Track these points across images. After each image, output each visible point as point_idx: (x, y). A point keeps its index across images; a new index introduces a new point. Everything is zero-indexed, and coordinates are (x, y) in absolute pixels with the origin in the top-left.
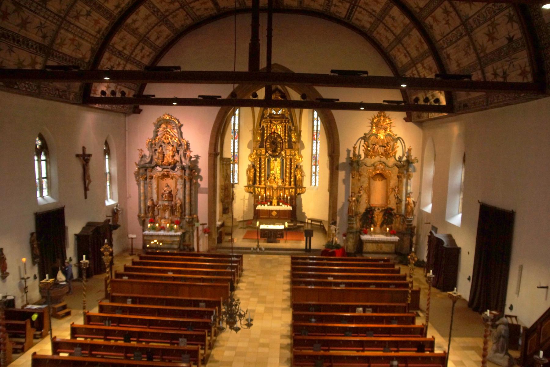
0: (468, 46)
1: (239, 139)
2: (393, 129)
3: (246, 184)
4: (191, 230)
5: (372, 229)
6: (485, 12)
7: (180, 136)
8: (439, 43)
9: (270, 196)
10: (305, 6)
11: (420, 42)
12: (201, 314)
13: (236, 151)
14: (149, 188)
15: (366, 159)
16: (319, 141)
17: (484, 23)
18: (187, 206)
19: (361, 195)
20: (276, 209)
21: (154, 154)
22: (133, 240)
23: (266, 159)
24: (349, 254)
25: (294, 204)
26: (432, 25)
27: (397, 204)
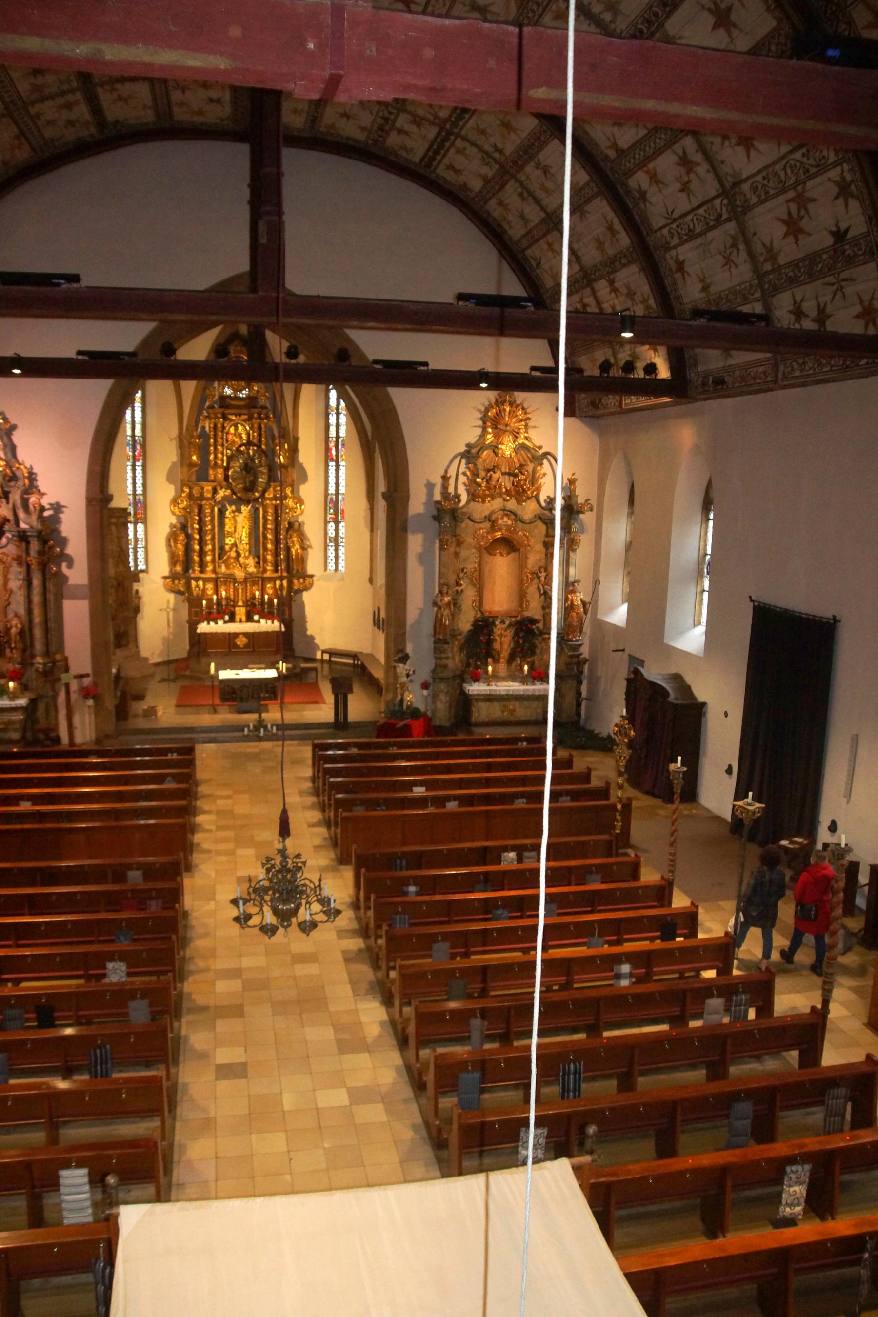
0: (734, 245)
1: (145, 460)
2: (532, 434)
3: (166, 573)
4: (50, 693)
5: (490, 668)
6: (785, 168)
7: (10, 455)
8: (659, 234)
9: (228, 598)
10: (323, 129)
11: (611, 228)
12: (140, 899)
13: (139, 491)
16: (342, 463)
17: (777, 195)
18: (38, 633)
19: (462, 591)
20: (244, 630)
23: (216, 509)
24: (440, 730)
25: (287, 616)
26: (645, 192)
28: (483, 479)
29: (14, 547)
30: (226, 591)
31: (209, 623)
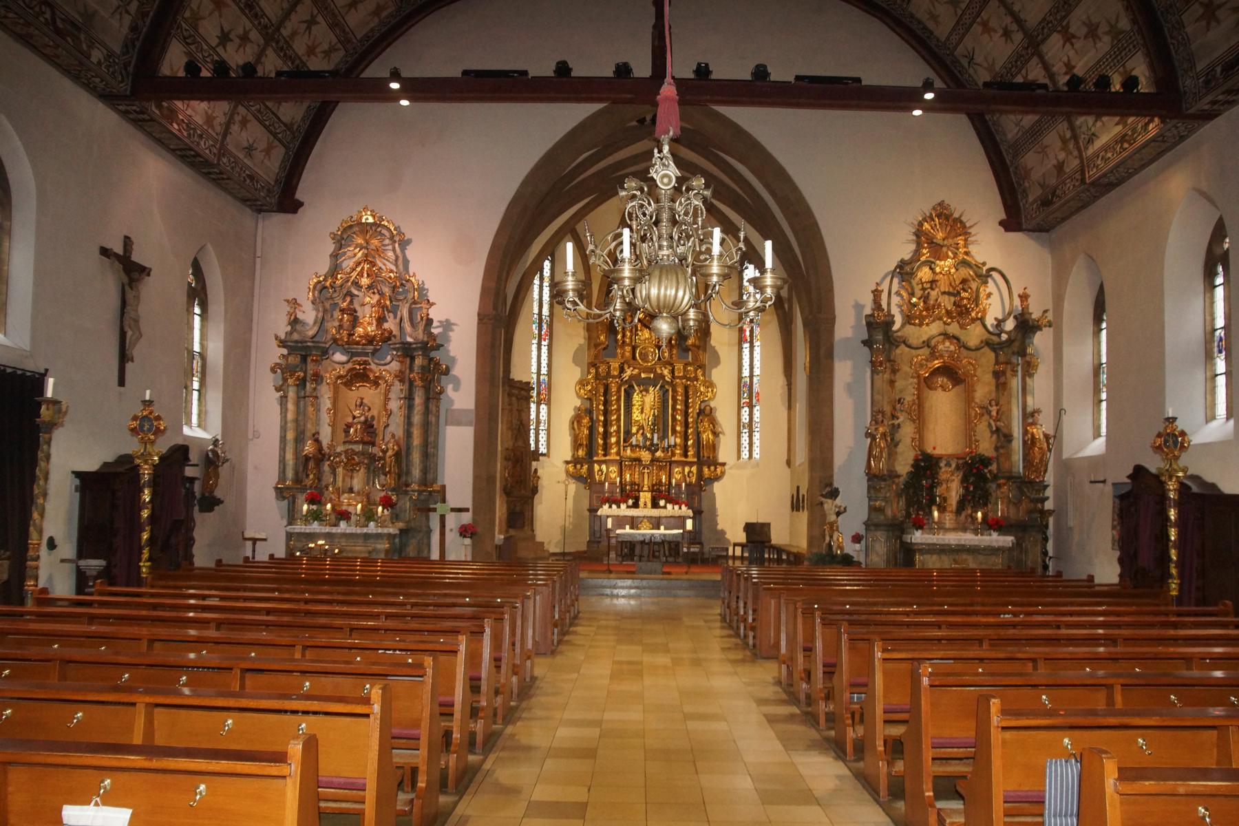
3: (569, 458)
9: (633, 483)
13: (544, 370)
14: (311, 409)
15: (910, 329)
16: (757, 344)
18: (416, 457)
19: (899, 425)
21: (328, 317)
22: (258, 542)
27: (997, 449)
28: (919, 299)
29: (398, 364)
30: (631, 475)
31: (610, 507)
